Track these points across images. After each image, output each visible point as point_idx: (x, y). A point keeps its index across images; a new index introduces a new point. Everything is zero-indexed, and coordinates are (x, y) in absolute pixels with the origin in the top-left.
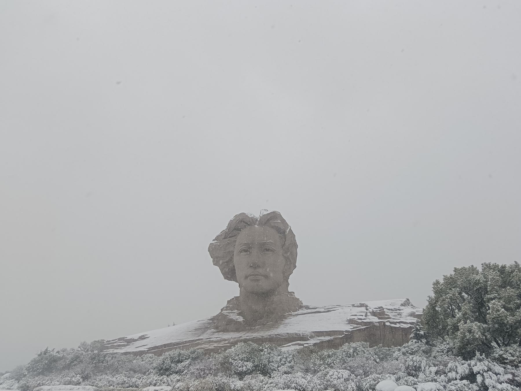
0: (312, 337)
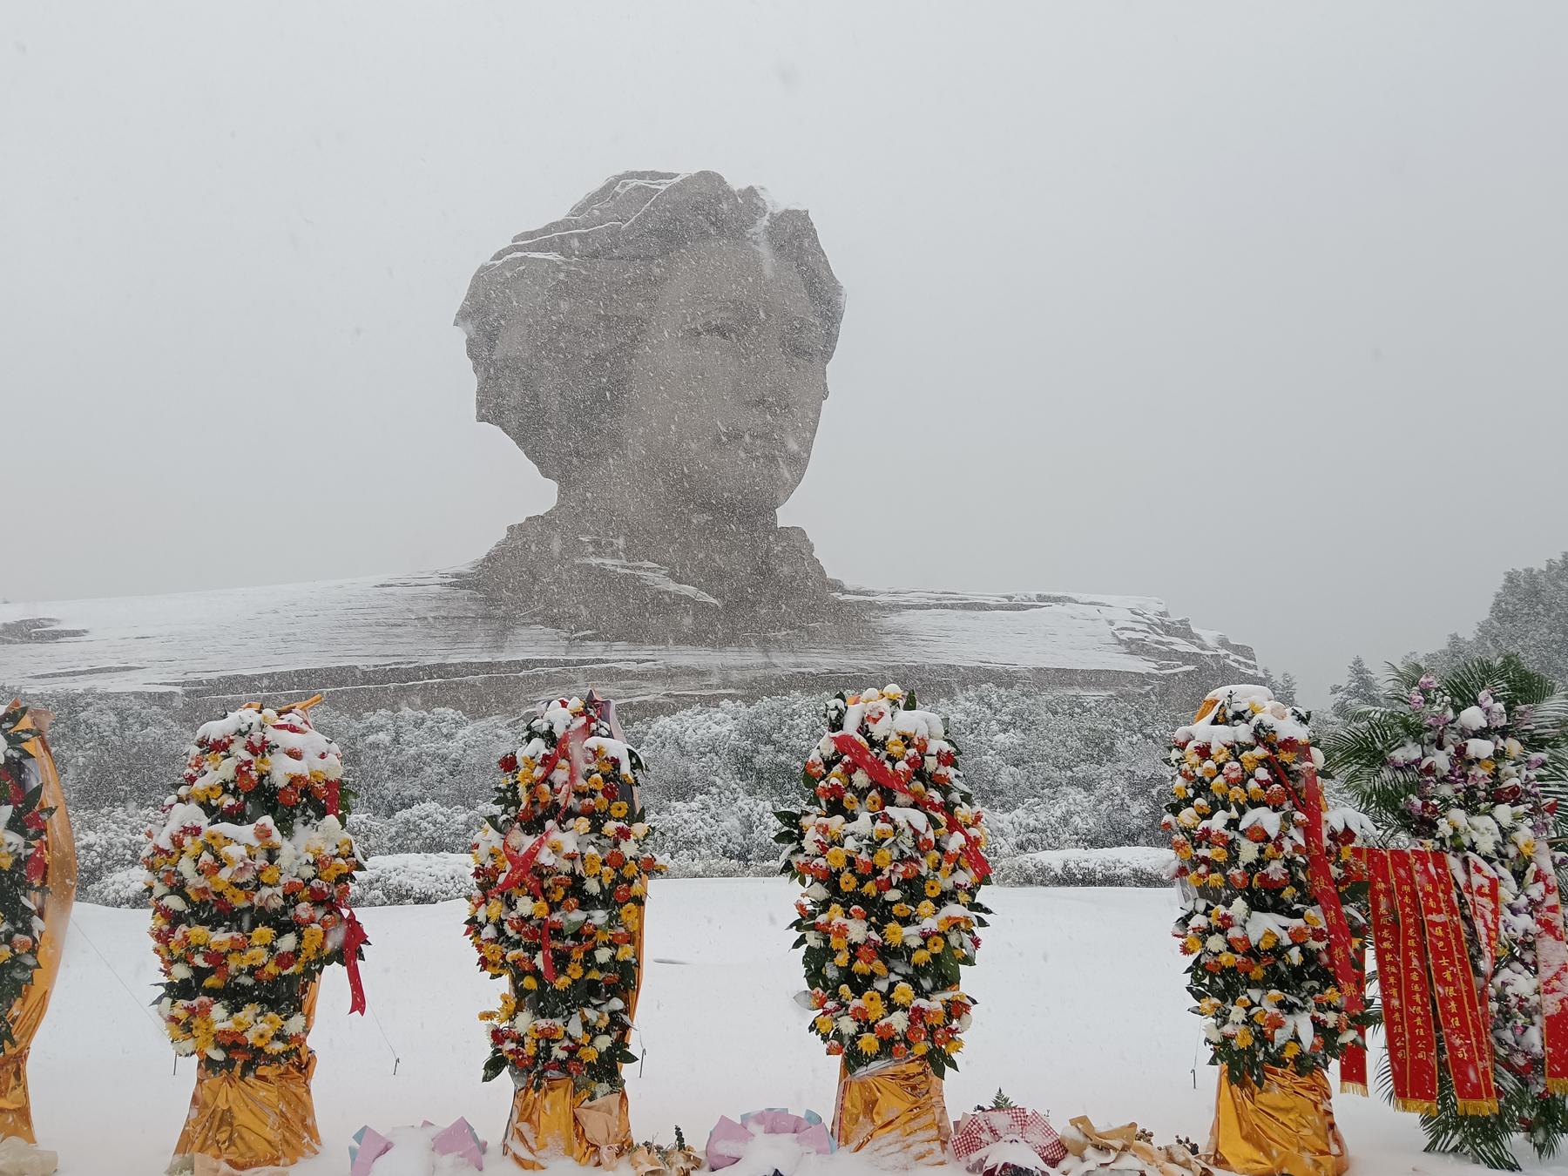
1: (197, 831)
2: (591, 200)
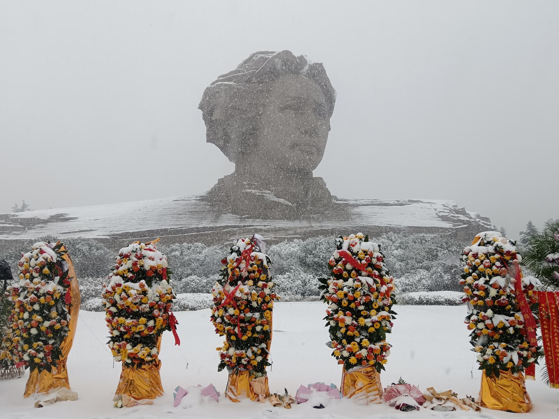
0: (410, 233)
1: (119, 285)
2: (246, 62)
